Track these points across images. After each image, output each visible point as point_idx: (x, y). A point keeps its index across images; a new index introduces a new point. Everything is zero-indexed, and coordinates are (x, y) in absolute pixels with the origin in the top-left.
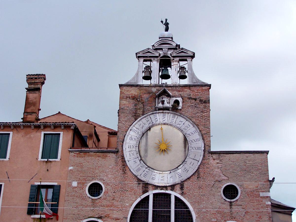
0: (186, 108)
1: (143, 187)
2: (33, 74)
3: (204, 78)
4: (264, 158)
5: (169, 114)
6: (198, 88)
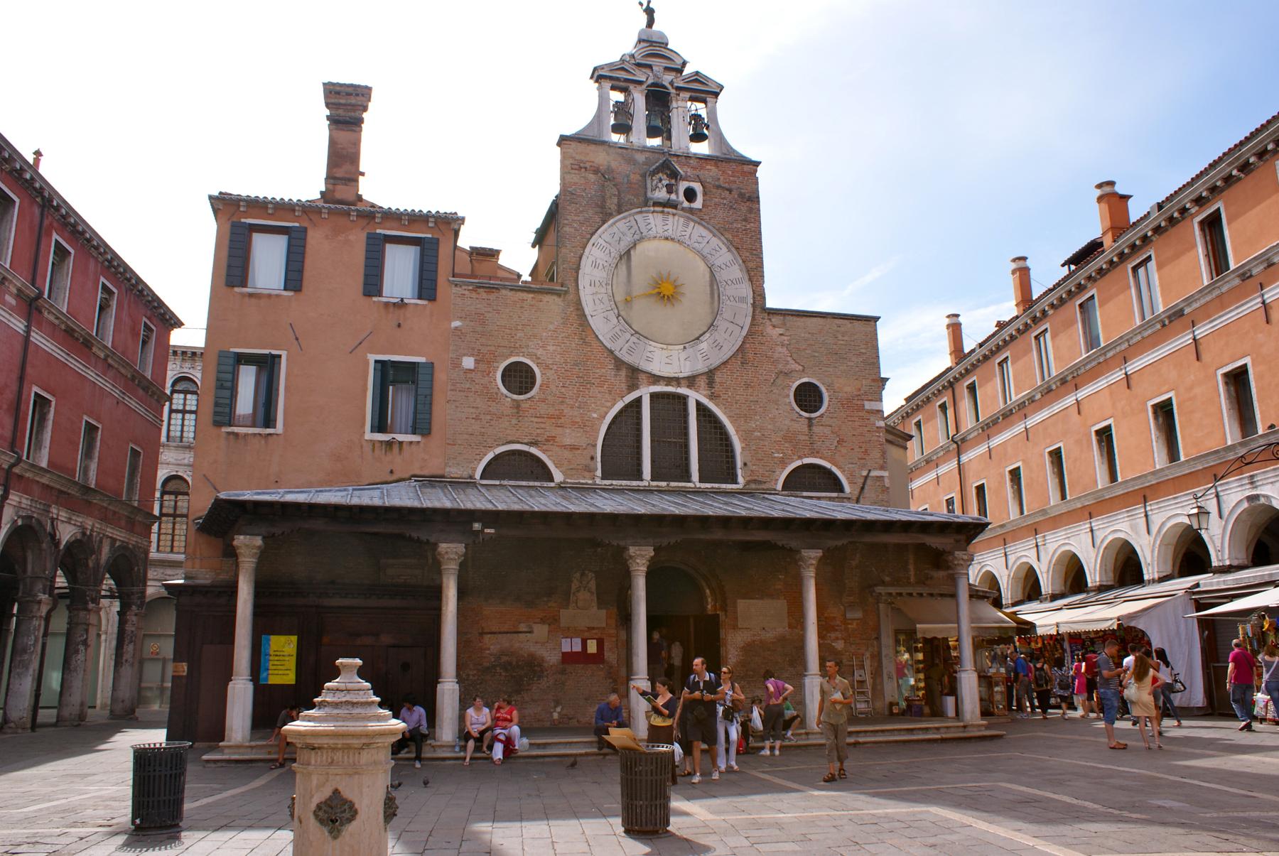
3: (743, 145)
5: (676, 218)
6: (734, 166)
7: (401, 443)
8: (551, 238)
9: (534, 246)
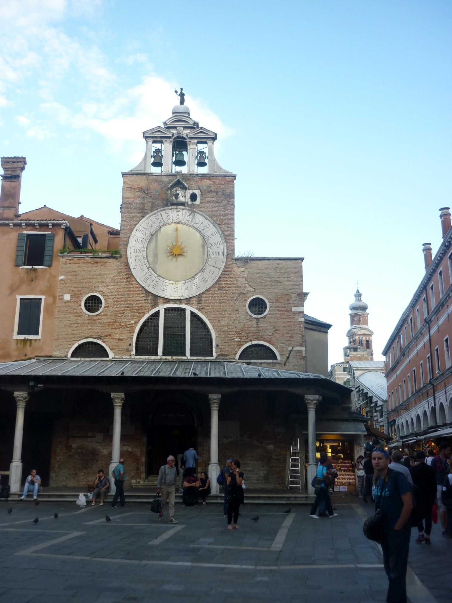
0: (205, 203)
2: (10, 156)
4: (298, 266)
5: (185, 211)
7: (31, 340)
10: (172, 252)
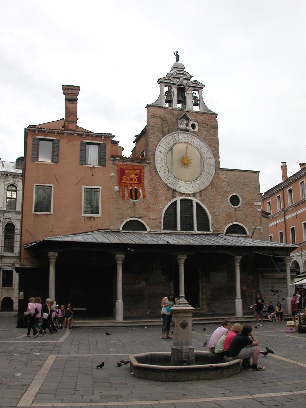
1: (172, 193)
5: (189, 135)
7: (94, 217)
8: (142, 141)
9: (134, 142)
10: (182, 161)
